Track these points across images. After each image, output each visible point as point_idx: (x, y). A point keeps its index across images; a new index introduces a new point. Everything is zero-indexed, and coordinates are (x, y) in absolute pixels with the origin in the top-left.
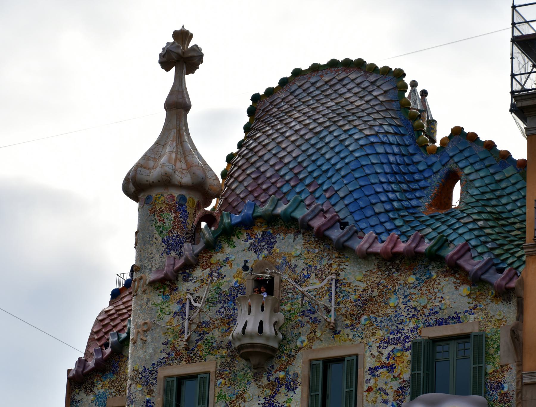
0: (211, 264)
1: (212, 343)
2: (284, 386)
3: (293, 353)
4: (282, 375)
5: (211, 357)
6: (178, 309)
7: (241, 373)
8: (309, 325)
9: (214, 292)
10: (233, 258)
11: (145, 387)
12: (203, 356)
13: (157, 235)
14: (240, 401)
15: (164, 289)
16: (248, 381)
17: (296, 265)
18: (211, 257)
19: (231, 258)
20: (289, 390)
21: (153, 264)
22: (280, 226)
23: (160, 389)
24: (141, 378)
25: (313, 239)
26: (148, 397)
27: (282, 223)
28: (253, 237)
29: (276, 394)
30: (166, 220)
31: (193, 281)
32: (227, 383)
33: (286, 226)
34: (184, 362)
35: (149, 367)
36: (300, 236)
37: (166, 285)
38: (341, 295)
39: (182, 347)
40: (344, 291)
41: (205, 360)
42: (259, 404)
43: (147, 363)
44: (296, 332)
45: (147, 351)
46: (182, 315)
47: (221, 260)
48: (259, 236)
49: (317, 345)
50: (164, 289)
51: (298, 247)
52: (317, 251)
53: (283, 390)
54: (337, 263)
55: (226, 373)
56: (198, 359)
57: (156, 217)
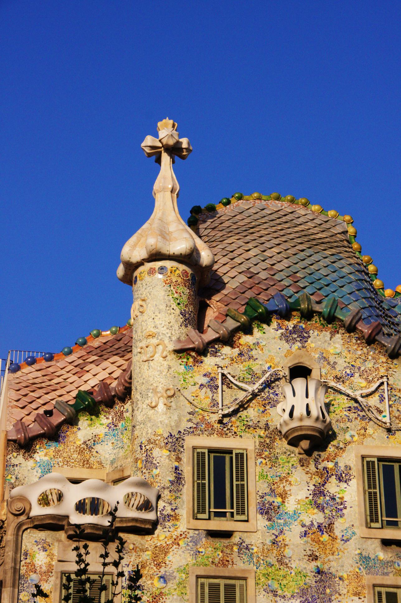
0: (240, 344)
1: (247, 421)
2: (334, 477)
3: (342, 445)
4: (330, 465)
5: (248, 435)
6: (206, 381)
7: (284, 457)
8: (357, 422)
9: (245, 372)
10: (264, 343)
11: (173, 453)
12: (238, 433)
13: (174, 306)
14: (284, 484)
15: (188, 359)
16: (293, 465)
17: (335, 363)
18: (240, 338)
19: (261, 342)
20: (340, 481)
21: (173, 333)
22: (314, 322)
23: (189, 458)
24: (167, 443)
25: (354, 341)
26: (177, 464)
27: (318, 320)
28: (284, 327)
29: (326, 483)
30: (182, 294)
31: (222, 357)
32: (268, 464)
33: (322, 324)
34: (216, 436)
35: (175, 433)
36: (338, 336)
37: (190, 355)
38: (393, 399)
39: (215, 419)
40: (395, 395)
41: (241, 436)
42: (308, 490)
43: (172, 430)
44: (342, 425)
45: (172, 417)
46: (211, 388)
47: (251, 343)
48: (290, 328)
49: (368, 441)
50: (188, 359)
51: (337, 345)
52: (359, 352)
53: (333, 479)
54: (385, 368)
55: (266, 453)
56: (233, 435)
57: (172, 288)
